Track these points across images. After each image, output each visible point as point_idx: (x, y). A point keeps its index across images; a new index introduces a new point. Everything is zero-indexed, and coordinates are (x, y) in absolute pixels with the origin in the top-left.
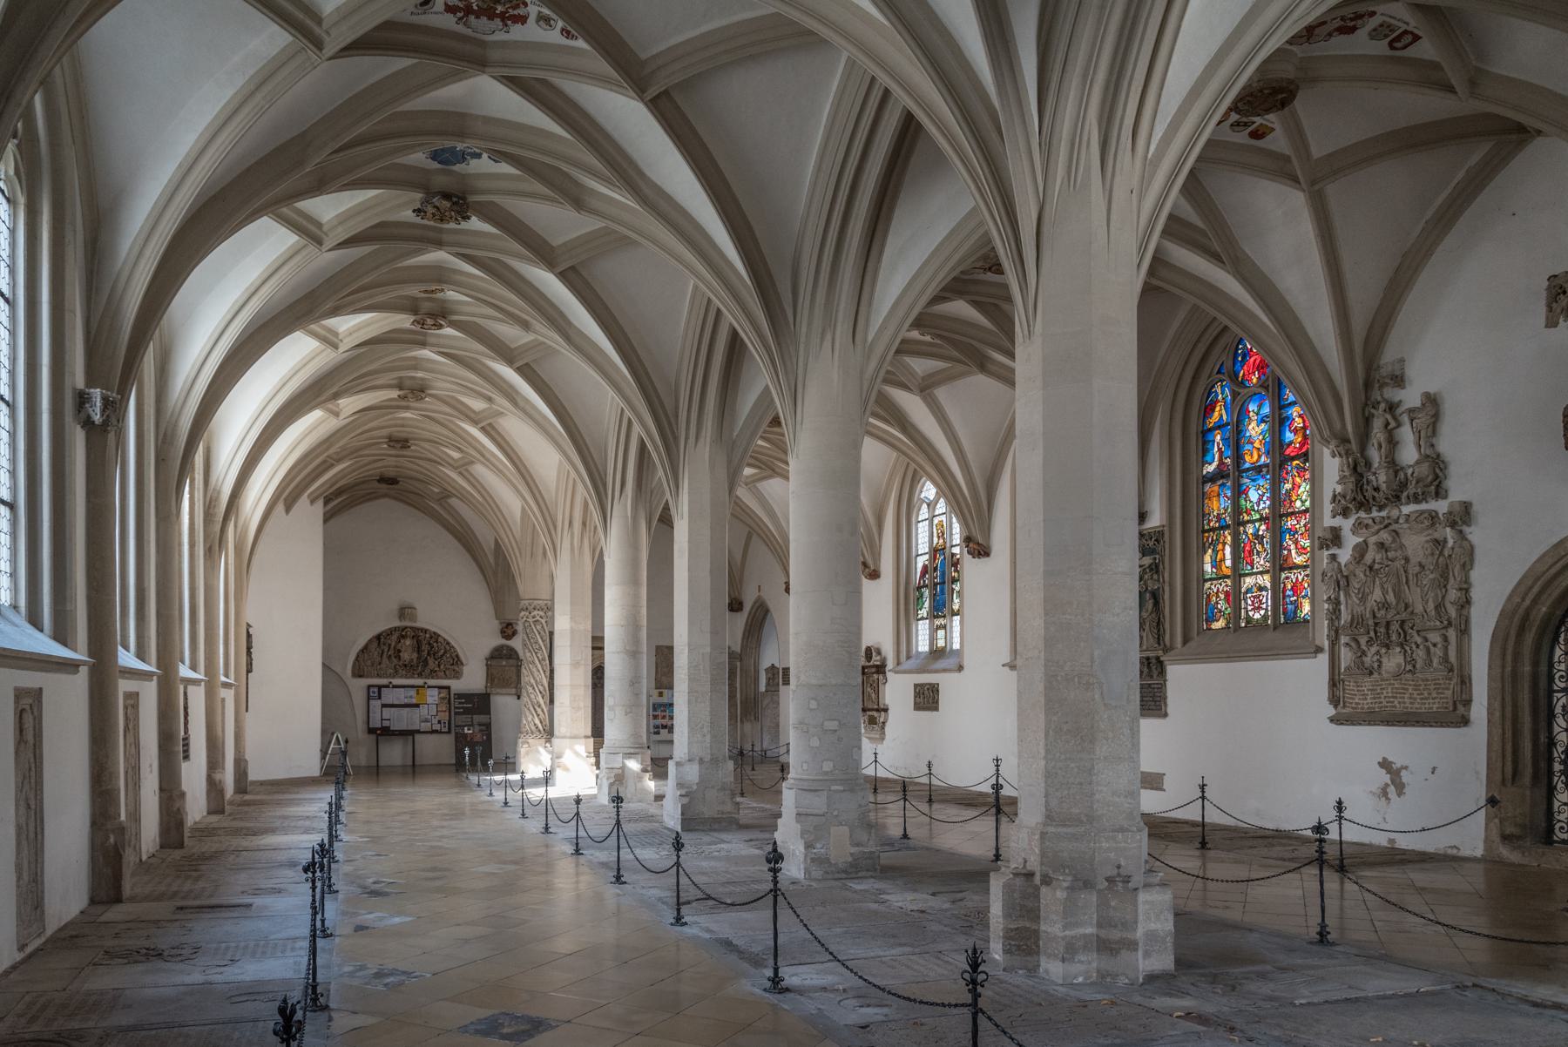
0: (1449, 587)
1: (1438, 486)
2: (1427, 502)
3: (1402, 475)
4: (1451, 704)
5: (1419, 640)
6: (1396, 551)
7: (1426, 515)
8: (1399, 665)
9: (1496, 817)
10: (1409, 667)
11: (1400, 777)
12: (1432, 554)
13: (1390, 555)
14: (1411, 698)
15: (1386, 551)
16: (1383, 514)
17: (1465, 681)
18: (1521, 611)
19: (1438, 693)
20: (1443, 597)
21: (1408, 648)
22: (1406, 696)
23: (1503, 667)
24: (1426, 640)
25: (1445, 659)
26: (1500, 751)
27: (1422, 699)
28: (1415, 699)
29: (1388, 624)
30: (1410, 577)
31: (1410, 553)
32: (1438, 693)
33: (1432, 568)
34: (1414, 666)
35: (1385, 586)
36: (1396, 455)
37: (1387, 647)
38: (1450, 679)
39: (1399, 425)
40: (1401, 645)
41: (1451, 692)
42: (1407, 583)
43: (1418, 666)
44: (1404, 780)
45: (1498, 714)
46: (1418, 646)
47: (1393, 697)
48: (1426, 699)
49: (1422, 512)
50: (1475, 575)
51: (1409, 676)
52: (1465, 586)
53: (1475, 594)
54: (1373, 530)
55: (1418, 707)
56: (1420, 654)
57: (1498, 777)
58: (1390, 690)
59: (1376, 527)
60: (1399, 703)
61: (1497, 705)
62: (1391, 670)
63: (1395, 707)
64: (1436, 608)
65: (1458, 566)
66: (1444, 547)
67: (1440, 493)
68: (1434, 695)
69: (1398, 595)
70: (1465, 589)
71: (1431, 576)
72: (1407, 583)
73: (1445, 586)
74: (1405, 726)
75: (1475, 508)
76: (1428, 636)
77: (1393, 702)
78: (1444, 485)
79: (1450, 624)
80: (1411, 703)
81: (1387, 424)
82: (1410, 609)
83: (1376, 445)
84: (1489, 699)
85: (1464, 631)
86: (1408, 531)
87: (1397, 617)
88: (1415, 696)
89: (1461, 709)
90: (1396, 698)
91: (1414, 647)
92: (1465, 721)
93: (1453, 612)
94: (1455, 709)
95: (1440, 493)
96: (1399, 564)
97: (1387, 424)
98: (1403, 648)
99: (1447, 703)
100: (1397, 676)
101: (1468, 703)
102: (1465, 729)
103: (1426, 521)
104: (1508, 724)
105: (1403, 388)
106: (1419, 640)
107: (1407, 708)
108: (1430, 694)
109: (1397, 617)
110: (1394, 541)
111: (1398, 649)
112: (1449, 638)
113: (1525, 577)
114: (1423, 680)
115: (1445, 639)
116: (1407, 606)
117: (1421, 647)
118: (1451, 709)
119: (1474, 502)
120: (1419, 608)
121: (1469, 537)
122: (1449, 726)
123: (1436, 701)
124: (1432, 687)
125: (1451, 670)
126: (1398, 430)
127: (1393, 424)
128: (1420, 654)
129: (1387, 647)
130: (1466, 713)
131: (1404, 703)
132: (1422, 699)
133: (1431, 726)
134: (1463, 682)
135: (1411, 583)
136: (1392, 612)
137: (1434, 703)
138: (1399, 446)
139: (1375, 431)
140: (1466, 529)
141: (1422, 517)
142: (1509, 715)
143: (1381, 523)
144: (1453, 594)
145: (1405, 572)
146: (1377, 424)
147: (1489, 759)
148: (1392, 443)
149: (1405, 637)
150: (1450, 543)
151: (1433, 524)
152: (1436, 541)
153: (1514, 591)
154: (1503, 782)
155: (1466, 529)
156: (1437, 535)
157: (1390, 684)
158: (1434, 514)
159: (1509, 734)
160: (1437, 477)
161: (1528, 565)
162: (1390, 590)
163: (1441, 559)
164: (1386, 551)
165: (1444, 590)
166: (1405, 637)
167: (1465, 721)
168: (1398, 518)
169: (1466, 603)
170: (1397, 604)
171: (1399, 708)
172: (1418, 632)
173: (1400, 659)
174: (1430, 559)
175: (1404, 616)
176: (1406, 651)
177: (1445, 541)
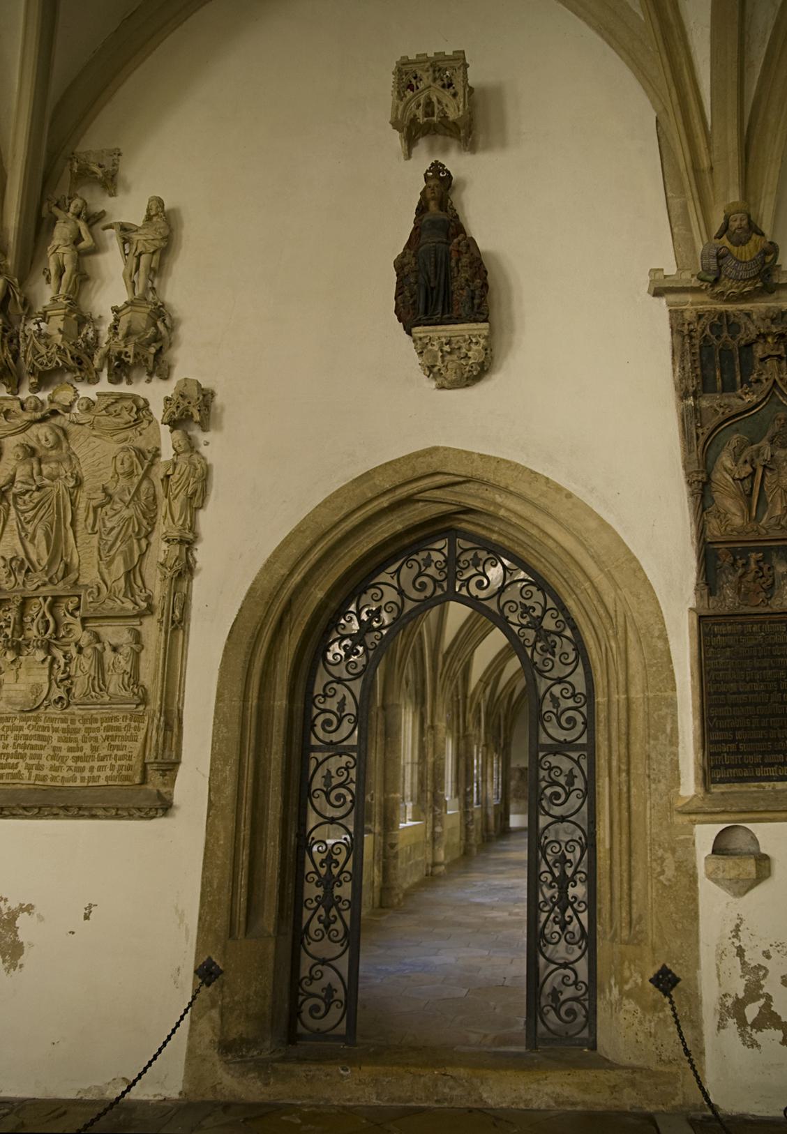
0: (153, 538)
1: (159, 351)
2: (129, 382)
3: (89, 331)
4: (138, 768)
5: (85, 638)
6: (59, 462)
7: (128, 403)
8: (36, 689)
9: (213, 1004)
10: (58, 693)
11: (15, 931)
12: (130, 474)
13: (46, 469)
14: (53, 758)
15: (40, 462)
16: (43, 396)
17: (171, 723)
18: (285, 594)
19: (111, 747)
20: (142, 555)
21: (59, 654)
22: (44, 753)
23: (245, 697)
24: (97, 638)
25: (134, 675)
26: (229, 867)
27: (77, 759)
28: (63, 759)
29: (24, 604)
30: (81, 514)
31: (85, 472)
32: (111, 747)
33: (128, 498)
34: (68, 691)
35: (30, 528)
36: (83, 295)
37: (18, 649)
38: (140, 718)
39: (95, 250)
40: (48, 647)
41: (139, 745)
42: (73, 524)
43: (77, 691)
44: (22, 937)
45: (229, 790)
46: (80, 650)
47: (16, 756)
48: (85, 759)
49: (122, 397)
50: (205, 519)
51: (54, 711)
52: (190, 536)
53: (201, 554)
54: (18, 422)
55: (68, 776)
56: (84, 667)
57: (221, 922)
58: (10, 741)
59: (27, 417)
60: (29, 768)
61: (229, 772)
62: (19, 699)
63: (18, 775)
64: (127, 574)
65: (182, 496)
66: (152, 464)
67: (159, 368)
68: (104, 752)
69: (56, 548)
70: (187, 542)
71: (126, 513)
72: (73, 524)
73: (146, 537)
74: (38, 816)
75: (218, 400)
76: (101, 631)
77: (16, 766)
78: (166, 356)
79: (150, 610)
80: (53, 768)
81: (78, 239)
82: (72, 577)
83: (53, 268)
84: (213, 760)
85: (177, 624)
86: (87, 429)
87: (44, 590)
88: (64, 753)
89: (155, 779)
90: (23, 757)
91: (73, 651)
92: (164, 806)
93: (156, 586)
94: (144, 780)
95: (159, 368)
96: (62, 486)
97: (78, 239)
98: (49, 652)
99: (129, 768)
100: (31, 710)
101: (170, 767)
102: (163, 820)
103: (125, 413)
104: (246, 811)
105: (111, 195)
106: (85, 638)
107: (44, 778)
108: (94, 749)
109: (44, 590)
110: (57, 445)
111: (40, 655)
112: (144, 637)
113: (298, 531)
114: (85, 721)
115: (137, 638)
116: (67, 569)
117: (88, 651)
118: (137, 780)
119: (217, 391)
120: (90, 576)
121: (203, 450)
122: (131, 817)
123: (107, 763)
124: (103, 734)
125: (144, 701)
126: (92, 258)
127: (87, 242)
128: (84, 667)
129: (18, 649)
130: (163, 790)
131: (39, 767)
132: (77, 759)
133: (94, 817)
134: (168, 726)
135: (80, 526)
136: (38, 578)
137: (100, 768)
138: (90, 284)
139: (56, 242)
140: (200, 436)
141: (118, 406)
142: (247, 792)
143: (35, 409)
144: (160, 550)
145: (73, 504)
146: (62, 232)
147: (206, 883)
148: (83, 278)
149: (56, 631)
150: (167, 454)
151: (137, 421)
152: (140, 453)
153: (276, 554)
154: (231, 934)
155: (200, 436)
156: (140, 443)
157: (12, 729)
158: (141, 403)
159: (245, 831)
160: (157, 338)
161: (309, 509)
162: (40, 533)
163: (145, 485)
164: (40, 462)
165: (144, 543)
166: (56, 631)
167: (164, 806)
168: (71, 406)
169: (184, 571)
170: (51, 563)
171: (27, 779)
172: (84, 620)
173: (42, 677)
174: (123, 482)
175: (60, 588)
176: (54, 659)
177: (157, 453)
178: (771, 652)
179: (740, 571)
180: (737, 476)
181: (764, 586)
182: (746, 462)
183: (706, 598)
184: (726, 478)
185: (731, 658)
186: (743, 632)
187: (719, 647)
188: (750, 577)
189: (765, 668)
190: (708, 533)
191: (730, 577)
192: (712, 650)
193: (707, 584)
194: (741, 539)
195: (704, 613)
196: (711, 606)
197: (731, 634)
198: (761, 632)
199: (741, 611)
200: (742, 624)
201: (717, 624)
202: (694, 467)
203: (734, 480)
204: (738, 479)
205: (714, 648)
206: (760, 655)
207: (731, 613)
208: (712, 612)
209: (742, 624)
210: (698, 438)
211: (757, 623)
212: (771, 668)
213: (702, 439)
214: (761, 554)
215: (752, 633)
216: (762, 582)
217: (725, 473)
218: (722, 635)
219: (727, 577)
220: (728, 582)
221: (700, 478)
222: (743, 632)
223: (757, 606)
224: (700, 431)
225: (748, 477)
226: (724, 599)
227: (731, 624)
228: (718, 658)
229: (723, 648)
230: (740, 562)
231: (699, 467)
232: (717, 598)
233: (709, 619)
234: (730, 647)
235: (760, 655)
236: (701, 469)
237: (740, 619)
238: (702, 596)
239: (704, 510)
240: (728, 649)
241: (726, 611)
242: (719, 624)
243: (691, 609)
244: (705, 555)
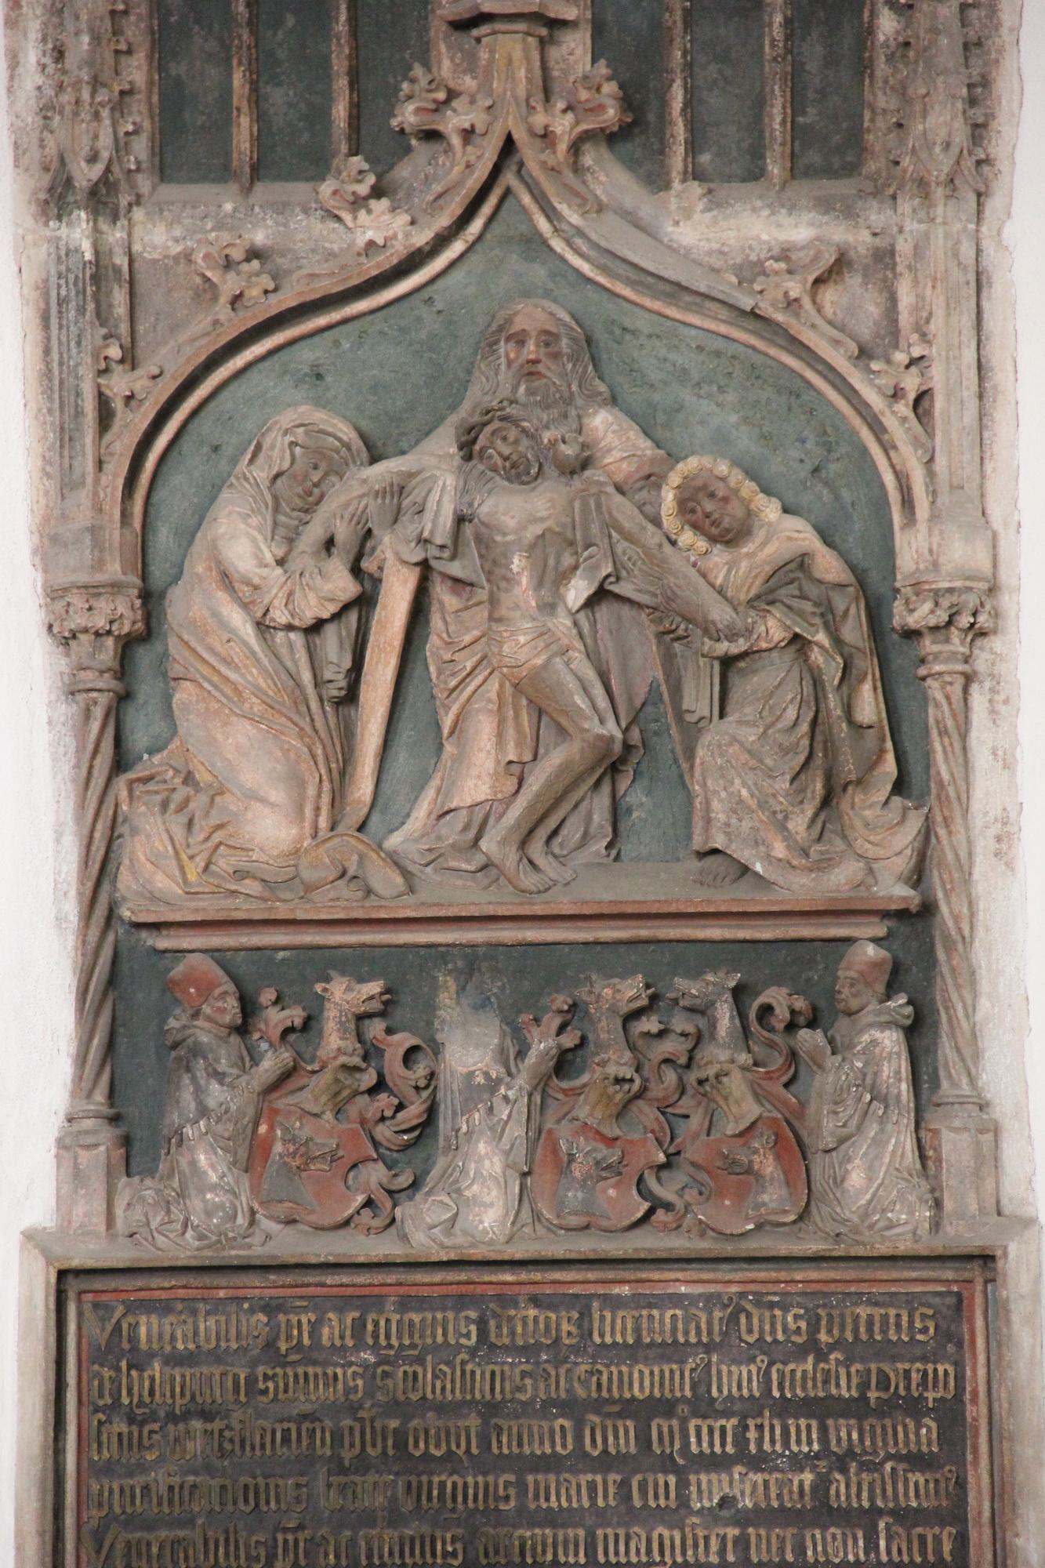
178: (401, 1444)
179: (270, 1063)
180: (280, 616)
181: (383, 1132)
182: (329, 544)
183: (98, 1184)
184: (224, 625)
185: (208, 1469)
186: (270, 1345)
187: (152, 1417)
188: (313, 1093)
189: (368, 1519)
190: (126, 882)
191: (216, 1093)
192: (120, 1426)
193: (115, 1119)
194: (282, 912)
195: (86, 1253)
196: (120, 1224)
197: (217, 1356)
198: (360, 1345)
199: (258, 1251)
200: (271, 1308)
201: (148, 1307)
202: (76, 567)
203: (263, 627)
204: (290, 627)
205: (131, 1420)
206: (347, 1455)
207: (209, 1257)
208: (121, 1254)
209: (271, 1308)
210: (105, 416)
211: (343, 1303)
212: (395, 1518)
213: (131, 425)
214: (374, 987)
215: (311, 1354)
216: (372, 1113)
217: (222, 596)
218: (174, 1360)
219: (198, 1091)
220: (203, 1111)
221: (101, 623)
222: (270, 1345)
223: (347, 1223)
224: (119, 384)
225: (336, 616)
226: (182, 1195)
227: (217, 1307)
228: (142, 1468)
229: (172, 1418)
230: (275, 1019)
231: (99, 565)
232: (149, 1189)
233: (114, 1283)
234: (206, 1416)
235: (347, 1455)
236: (114, 569)
237: (256, 1286)
238: (78, 1176)
239: (120, 764)
240: (197, 1424)
241: (186, 1248)
242: (164, 1308)
243: (31, 1237)
244: (112, 980)
